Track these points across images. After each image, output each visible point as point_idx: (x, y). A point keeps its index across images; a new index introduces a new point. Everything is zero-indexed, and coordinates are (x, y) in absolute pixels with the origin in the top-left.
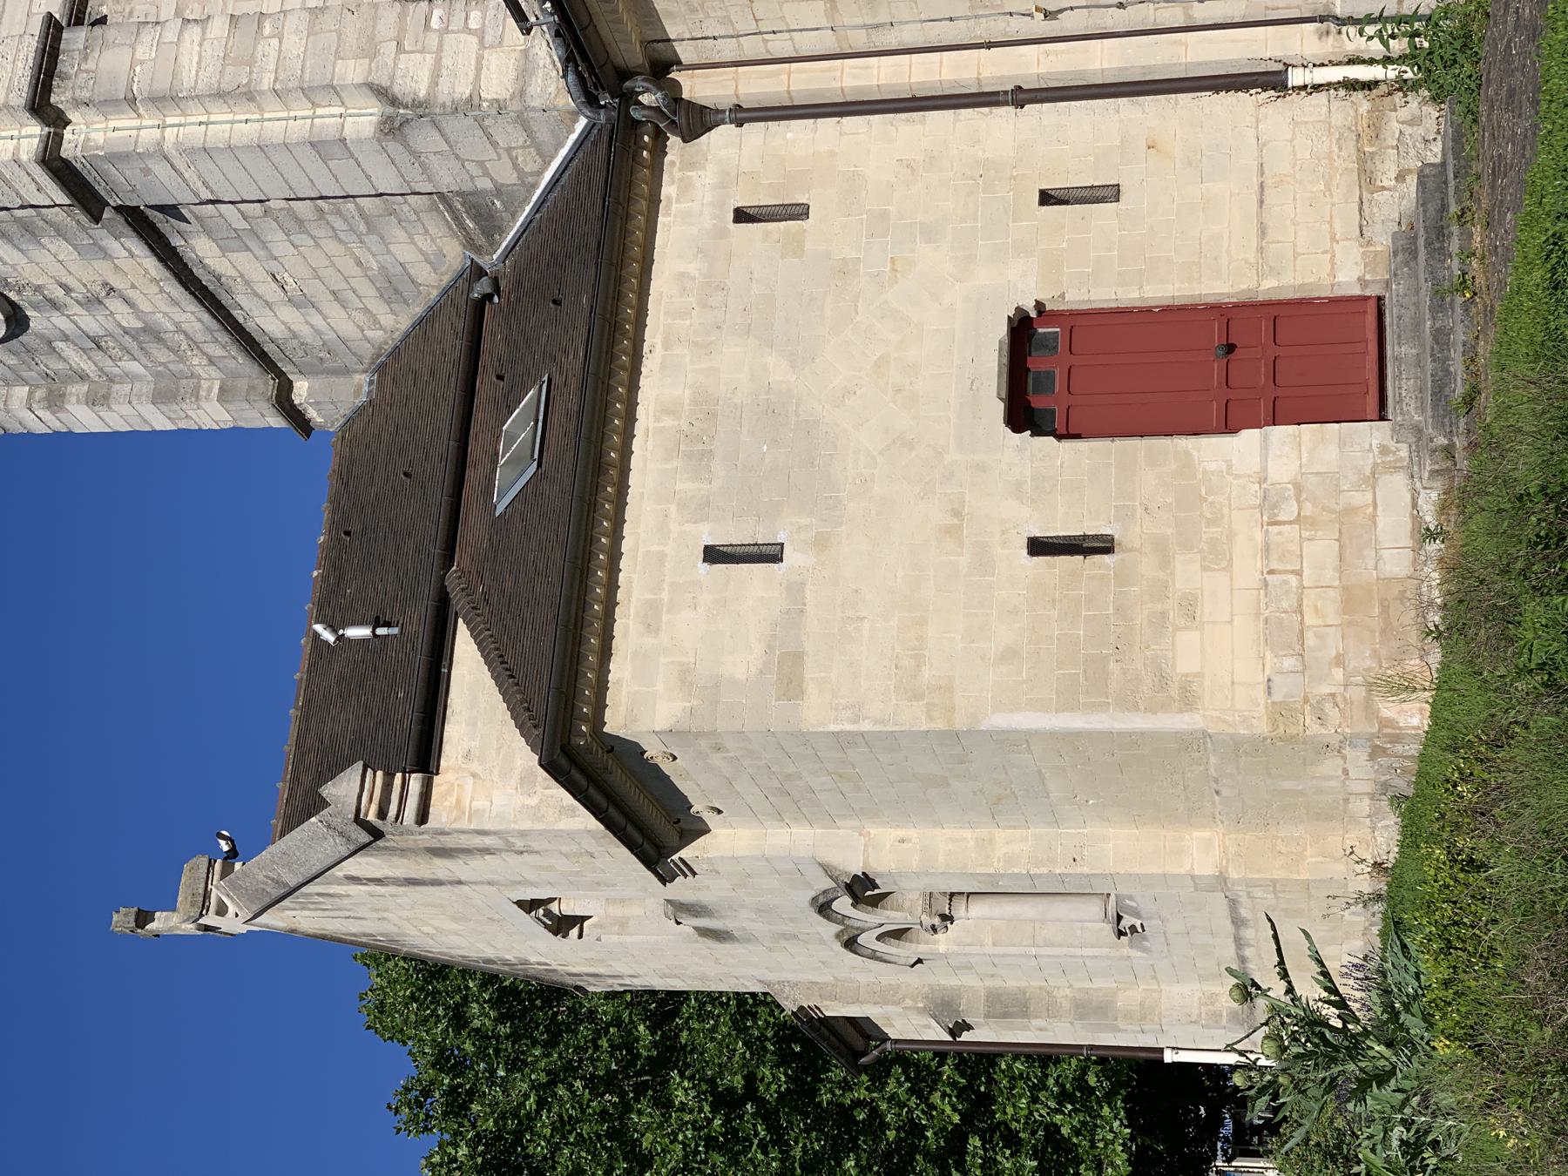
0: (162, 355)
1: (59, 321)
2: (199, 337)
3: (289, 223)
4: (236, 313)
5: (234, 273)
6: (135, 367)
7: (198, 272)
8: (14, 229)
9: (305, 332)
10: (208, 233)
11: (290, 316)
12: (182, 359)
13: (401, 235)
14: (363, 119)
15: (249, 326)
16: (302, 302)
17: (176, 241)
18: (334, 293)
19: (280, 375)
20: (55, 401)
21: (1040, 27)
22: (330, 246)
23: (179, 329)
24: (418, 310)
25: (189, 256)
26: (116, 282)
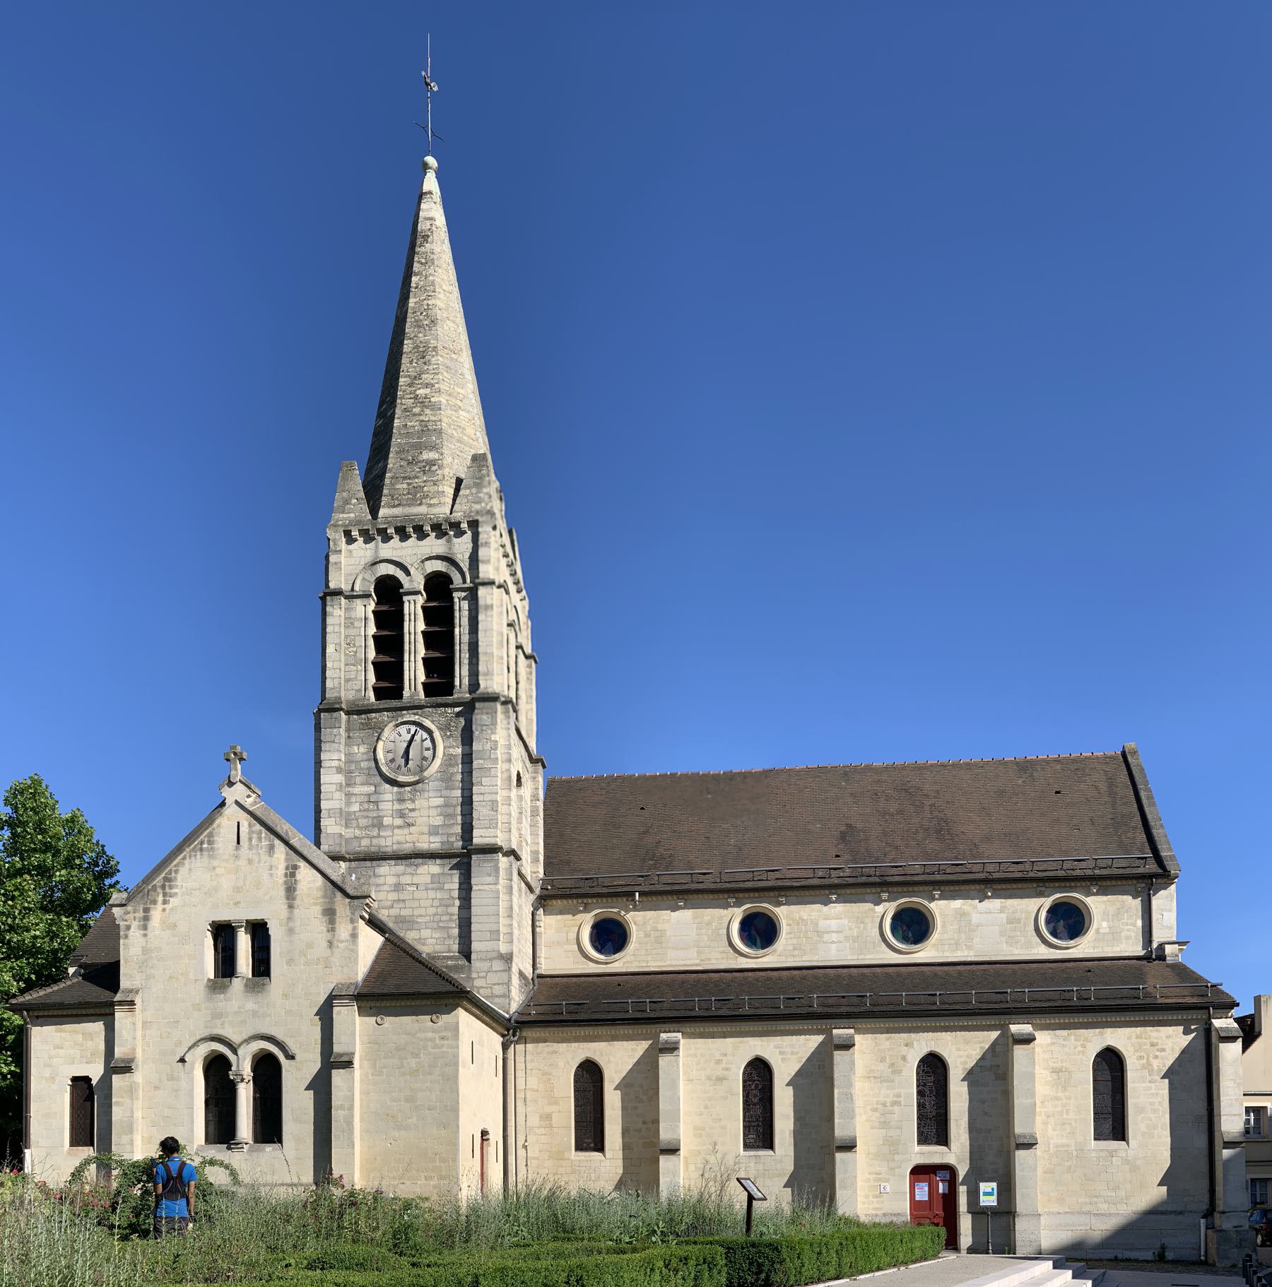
0: (363, 822)
1: (388, 797)
2: (375, 841)
3: (445, 902)
4: (393, 862)
5: (419, 871)
6: (355, 808)
7: (420, 861)
8: (450, 810)
9: (381, 880)
10: (443, 874)
11: (391, 880)
12: (358, 827)
13: (437, 935)
14: (503, 949)
15: (384, 863)
16: (398, 887)
17: (438, 861)
18: (404, 901)
19: (350, 860)
20: (339, 770)
21: (520, 1144)
22: (432, 911)
23: (379, 836)
24: (391, 925)
25: (430, 862)
26: (412, 829)
